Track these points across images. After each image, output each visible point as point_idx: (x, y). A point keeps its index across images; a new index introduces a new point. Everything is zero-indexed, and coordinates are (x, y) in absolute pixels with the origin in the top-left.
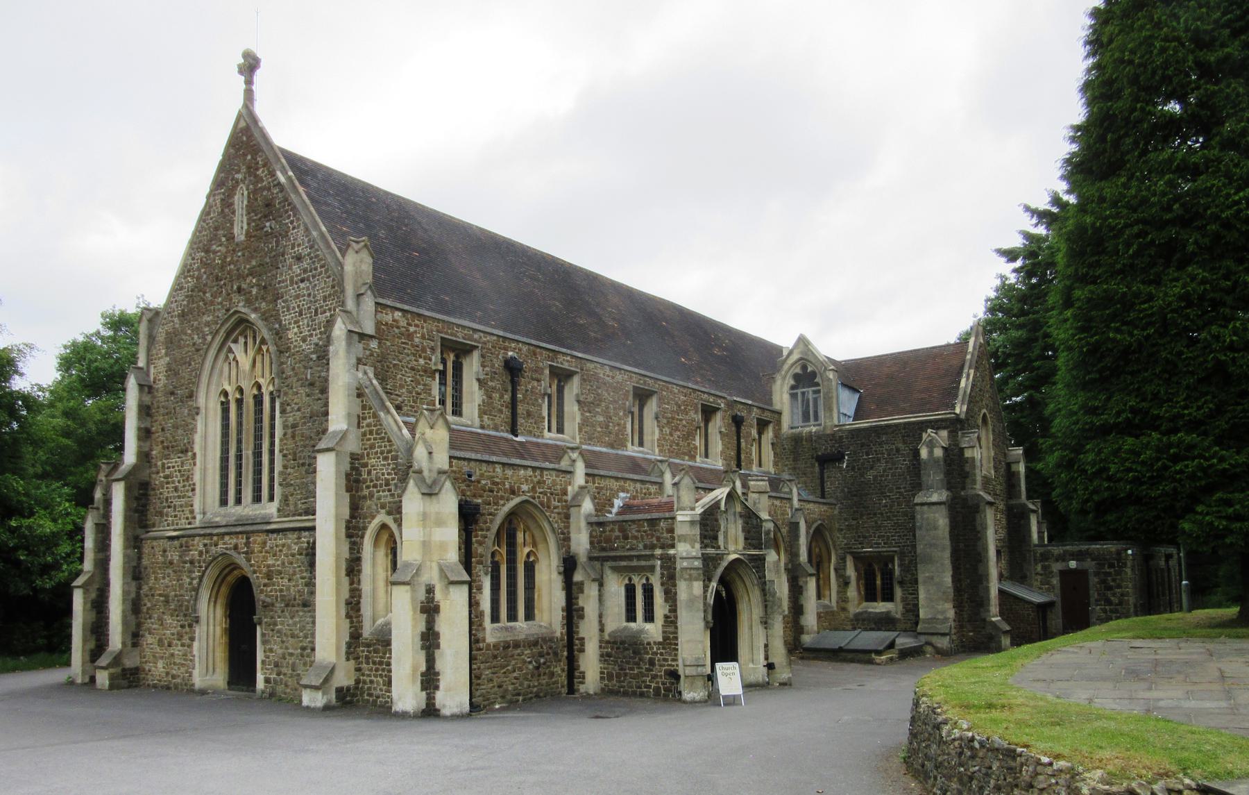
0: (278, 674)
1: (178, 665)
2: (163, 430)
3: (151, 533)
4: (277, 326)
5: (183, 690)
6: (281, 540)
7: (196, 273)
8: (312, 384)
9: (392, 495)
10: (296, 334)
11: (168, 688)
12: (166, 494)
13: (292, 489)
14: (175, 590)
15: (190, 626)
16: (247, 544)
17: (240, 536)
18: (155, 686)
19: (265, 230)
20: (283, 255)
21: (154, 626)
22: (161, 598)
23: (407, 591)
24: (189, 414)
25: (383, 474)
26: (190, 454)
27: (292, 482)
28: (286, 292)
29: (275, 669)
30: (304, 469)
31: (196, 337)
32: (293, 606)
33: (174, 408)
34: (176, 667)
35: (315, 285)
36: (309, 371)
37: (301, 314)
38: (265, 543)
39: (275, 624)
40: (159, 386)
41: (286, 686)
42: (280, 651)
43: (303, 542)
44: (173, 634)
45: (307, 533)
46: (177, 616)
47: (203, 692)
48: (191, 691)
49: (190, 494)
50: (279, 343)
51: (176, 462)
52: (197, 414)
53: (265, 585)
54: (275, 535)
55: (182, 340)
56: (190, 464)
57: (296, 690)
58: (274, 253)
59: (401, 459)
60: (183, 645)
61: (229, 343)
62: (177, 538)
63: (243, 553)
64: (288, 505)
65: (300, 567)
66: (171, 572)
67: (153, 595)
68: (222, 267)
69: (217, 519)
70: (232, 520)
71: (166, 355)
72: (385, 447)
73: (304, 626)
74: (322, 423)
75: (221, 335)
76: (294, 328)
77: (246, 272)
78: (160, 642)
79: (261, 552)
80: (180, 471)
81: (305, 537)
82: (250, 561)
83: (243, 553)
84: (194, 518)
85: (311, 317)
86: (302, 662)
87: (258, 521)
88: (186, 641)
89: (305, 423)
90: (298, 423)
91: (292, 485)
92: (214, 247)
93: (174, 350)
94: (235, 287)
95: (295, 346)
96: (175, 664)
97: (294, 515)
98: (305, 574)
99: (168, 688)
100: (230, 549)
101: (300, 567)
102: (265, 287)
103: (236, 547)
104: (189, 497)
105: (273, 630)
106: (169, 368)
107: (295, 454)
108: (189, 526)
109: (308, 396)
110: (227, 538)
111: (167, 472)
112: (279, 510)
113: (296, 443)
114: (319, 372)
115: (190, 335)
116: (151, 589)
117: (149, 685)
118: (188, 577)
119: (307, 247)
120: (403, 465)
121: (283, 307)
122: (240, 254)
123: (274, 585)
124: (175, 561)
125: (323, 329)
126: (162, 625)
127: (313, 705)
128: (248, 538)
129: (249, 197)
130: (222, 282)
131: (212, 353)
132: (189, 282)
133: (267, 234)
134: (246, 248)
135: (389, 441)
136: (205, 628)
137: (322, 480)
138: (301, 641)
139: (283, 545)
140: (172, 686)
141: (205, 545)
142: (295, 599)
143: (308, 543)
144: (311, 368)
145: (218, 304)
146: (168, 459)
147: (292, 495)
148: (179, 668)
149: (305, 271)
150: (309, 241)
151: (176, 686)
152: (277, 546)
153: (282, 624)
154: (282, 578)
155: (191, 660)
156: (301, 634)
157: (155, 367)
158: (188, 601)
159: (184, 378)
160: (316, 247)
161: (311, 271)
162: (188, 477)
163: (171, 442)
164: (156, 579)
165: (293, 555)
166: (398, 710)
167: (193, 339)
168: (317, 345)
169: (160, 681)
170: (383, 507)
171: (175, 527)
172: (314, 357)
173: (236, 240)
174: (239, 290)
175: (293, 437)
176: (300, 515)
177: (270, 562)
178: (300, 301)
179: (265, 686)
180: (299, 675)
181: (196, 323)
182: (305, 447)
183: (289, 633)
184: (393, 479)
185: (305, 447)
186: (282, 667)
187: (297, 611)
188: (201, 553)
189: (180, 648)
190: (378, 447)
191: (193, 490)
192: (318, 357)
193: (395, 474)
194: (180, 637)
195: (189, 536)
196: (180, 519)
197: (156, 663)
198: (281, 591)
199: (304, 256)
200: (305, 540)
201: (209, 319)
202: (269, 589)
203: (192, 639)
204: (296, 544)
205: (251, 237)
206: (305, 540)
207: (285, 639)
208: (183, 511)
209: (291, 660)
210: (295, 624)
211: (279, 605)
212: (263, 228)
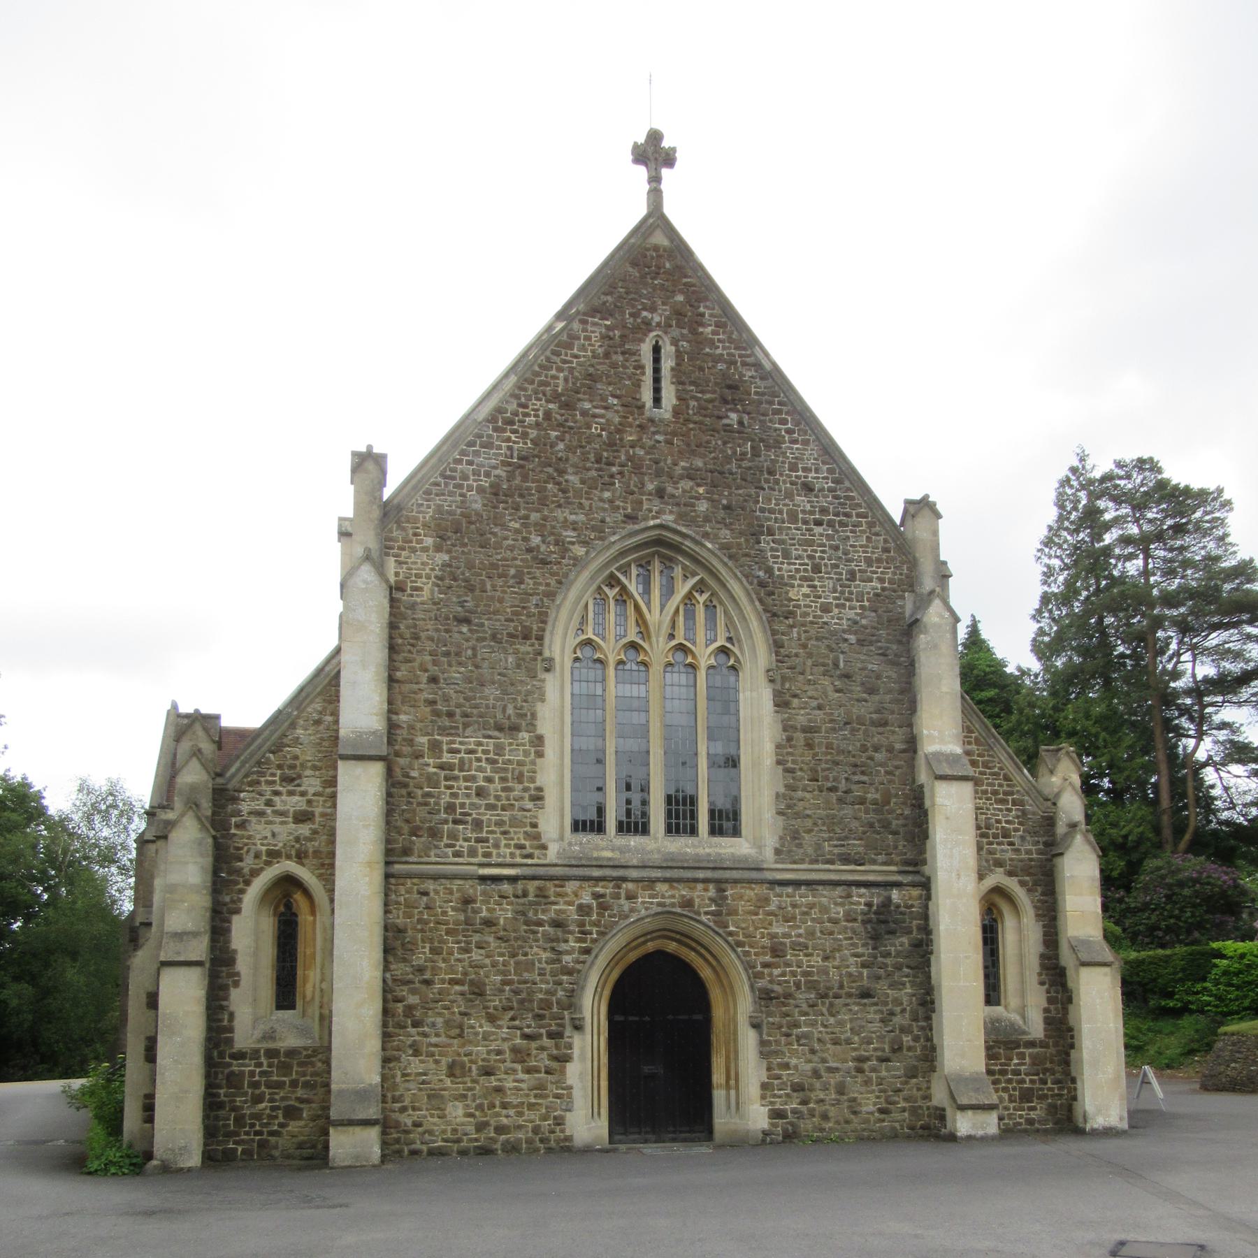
0: (804, 1102)
1: (516, 1106)
2: (433, 680)
3: (397, 866)
4: (761, 574)
5: (537, 1150)
6: (804, 897)
7: (533, 433)
8: (847, 676)
9: (1017, 851)
10: (807, 596)
11: (485, 1151)
12: (446, 799)
13: (809, 823)
14: (504, 973)
15: (555, 1036)
16: (720, 899)
17: (700, 886)
18: (435, 1153)
19: (725, 421)
20: (771, 473)
21: (434, 1040)
22: (457, 988)
23: (1105, 975)
24: (518, 666)
25: (998, 821)
26: (524, 736)
27: (808, 812)
28: (780, 528)
29: (795, 1094)
30: (833, 797)
31: (536, 540)
32: (837, 996)
33: (474, 649)
34: (512, 1112)
35: (848, 537)
36: (841, 656)
37: (816, 569)
38: (767, 900)
39: (796, 1025)
40: (419, 600)
41: (825, 1117)
42: (809, 1066)
43: (859, 903)
44: (499, 1053)
45: (863, 890)
46: (513, 1019)
47: (587, 1151)
48: (566, 1149)
49: (529, 805)
50: (769, 600)
51: (480, 744)
52: (547, 670)
53: (765, 965)
54: (790, 890)
55: (494, 534)
56: (526, 753)
57: (847, 1122)
58: (745, 464)
59: (1031, 805)
60: (528, 1071)
61: (613, 569)
62: (513, 880)
63: (706, 913)
64: (800, 846)
65: (852, 938)
66: (491, 939)
67: (428, 983)
68: (611, 444)
69: (608, 854)
70: (656, 858)
71: (438, 549)
72: (1000, 785)
73: (863, 1027)
74: (873, 736)
75: (612, 551)
76: (800, 586)
77: (678, 471)
78: (454, 1070)
79: (757, 914)
80: (492, 762)
81: (860, 896)
82: (727, 927)
83: (706, 913)
84: (544, 847)
85: (839, 580)
86: (859, 1080)
87: (728, 864)
88: (544, 1060)
89: (834, 729)
90: (820, 727)
91: (808, 816)
92: (587, 405)
93: (465, 545)
94: (650, 487)
95: (805, 615)
96: (505, 1106)
97: (816, 861)
98: (860, 950)
99: (485, 1151)
100: (673, 905)
101: (852, 938)
102: (727, 508)
103: (688, 903)
104: (529, 810)
105: (788, 1035)
106: (447, 579)
107: (814, 771)
108: (529, 861)
109: (838, 691)
110: (662, 888)
111: (446, 758)
112: (778, 852)
113: (815, 755)
114: (863, 662)
115: (517, 531)
116: (421, 970)
117: (414, 1153)
118: (545, 949)
119: (826, 478)
120: (1034, 813)
121: (772, 549)
122: (657, 437)
123: (788, 965)
124: (502, 921)
125: (866, 603)
126: (461, 1036)
127: (980, 1133)
128: (721, 890)
129: (679, 355)
130: (614, 469)
131: (586, 575)
132: (508, 440)
133: (728, 428)
134: (674, 434)
135: (1006, 778)
136: (589, 1037)
137: (947, 818)
138: (855, 1049)
139: (811, 906)
140: (498, 1146)
141: (597, 896)
142: (841, 987)
143: (869, 905)
144: (843, 652)
145: (602, 500)
146: (451, 735)
147: (810, 831)
148: (520, 1114)
149: (824, 511)
150: (830, 471)
151: (512, 1148)
152: (794, 906)
153: (813, 1024)
154: (806, 955)
155: (557, 1096)
156: (856, 1038)
157: (400, 563)
158: (550, 993)
159: (501, 601)
160: (847, 484)
161: (837, 515)
162: (521, 774)
163: (459, 706)
164: (434, 951)
165: (835, 922)
166: (1096, 1126)
167: (526, 539)
168: (856, 623)
169: (458, 1141)
170: (999, 863)
171: (480, 859)
172: (852, 638)
173: (647, 414)
174: (660, 493)
175: (809, 745)
176: (831, 862)
177: (778, 929)
178: (816, 551)
179: (773, 1125)
180: (854, 1100)
181: (535, 516)
182: (837, 764)
183: (827, 1037)
184: (1016, 830)
185: (837, 764)
186: (811, 1090)
187: (847, 1005)
188: (583, 910)
189: (521, 1076)
190: (988, 785)
191: (538, 798)
192: (860, 642)
193: (1020, 823)
194: (519, 1055)
195: (551, 878)
196: (497, 846)
197: (445, 1110)
198: (805, 974)
199: (822, 490)
200: (862, 900)
201: (573, 517)
202: (776, 972)
203: (566, 1059)
204: (842, 905)
205: (687, 420)
206: (862, 900)
207: (817, 1046)
208: (505, 833)
209: (833, 1080)
210: (841, 1023)
211: (802, 997)
212: (720, 418)
